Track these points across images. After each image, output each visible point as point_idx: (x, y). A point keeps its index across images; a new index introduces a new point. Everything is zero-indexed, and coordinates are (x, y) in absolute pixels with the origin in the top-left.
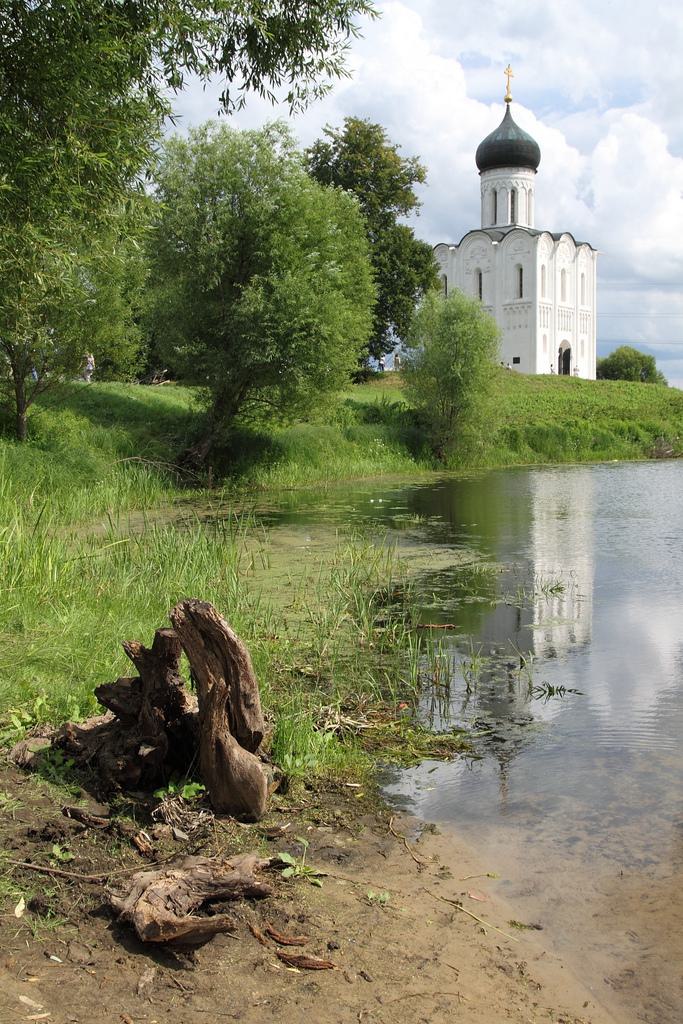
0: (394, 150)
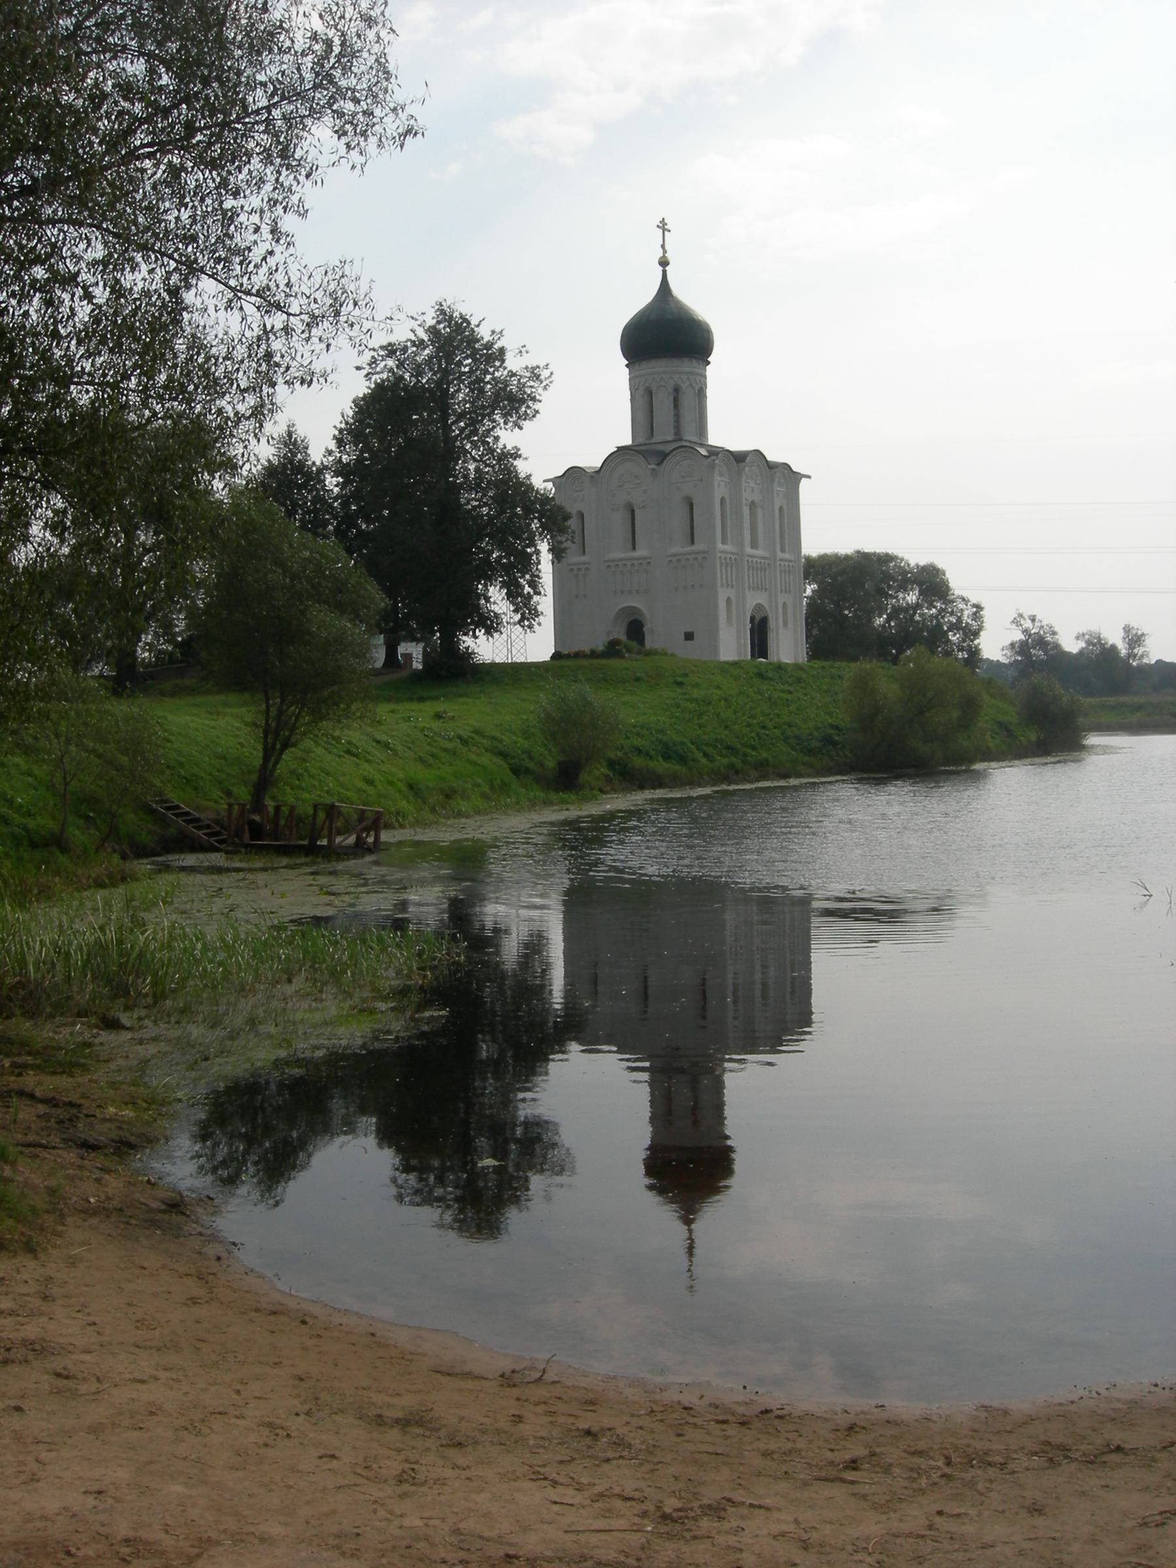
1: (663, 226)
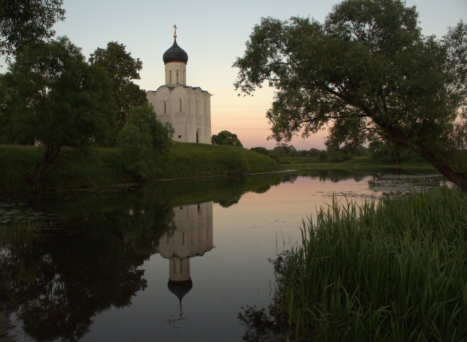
1: (175, 27)
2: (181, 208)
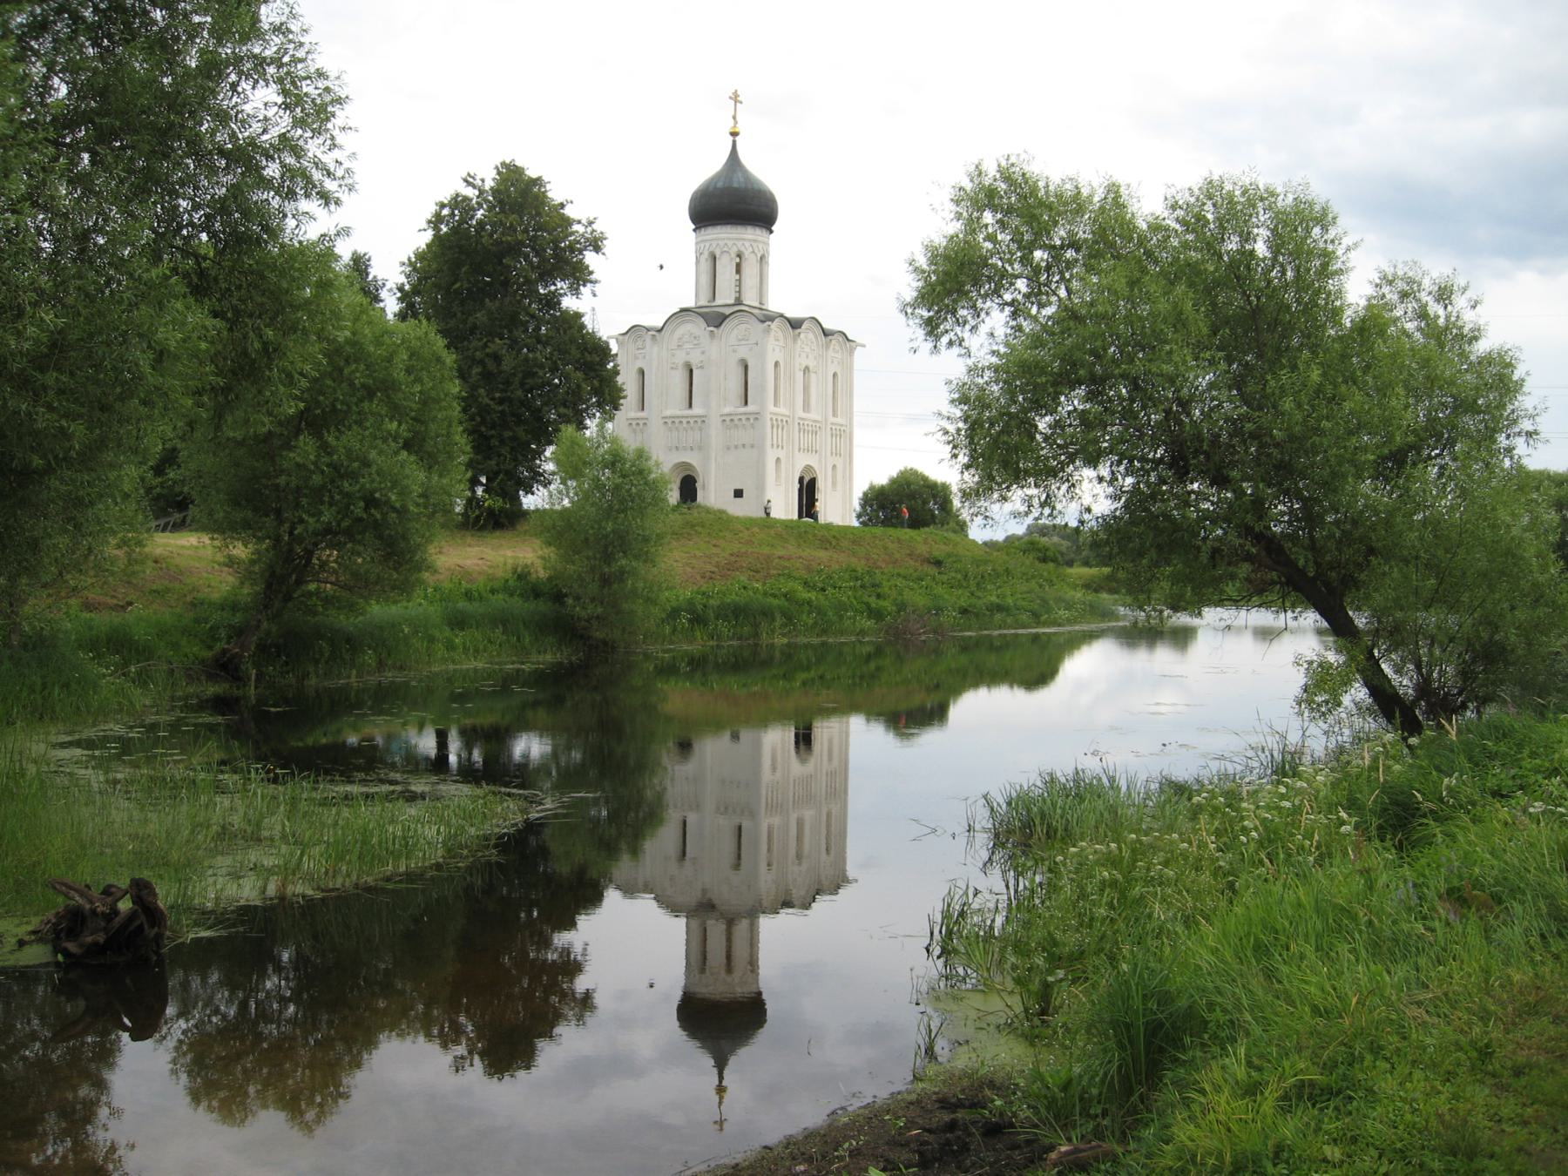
0: (562, 206)
1: (735, 98)
2: (735, 737)
